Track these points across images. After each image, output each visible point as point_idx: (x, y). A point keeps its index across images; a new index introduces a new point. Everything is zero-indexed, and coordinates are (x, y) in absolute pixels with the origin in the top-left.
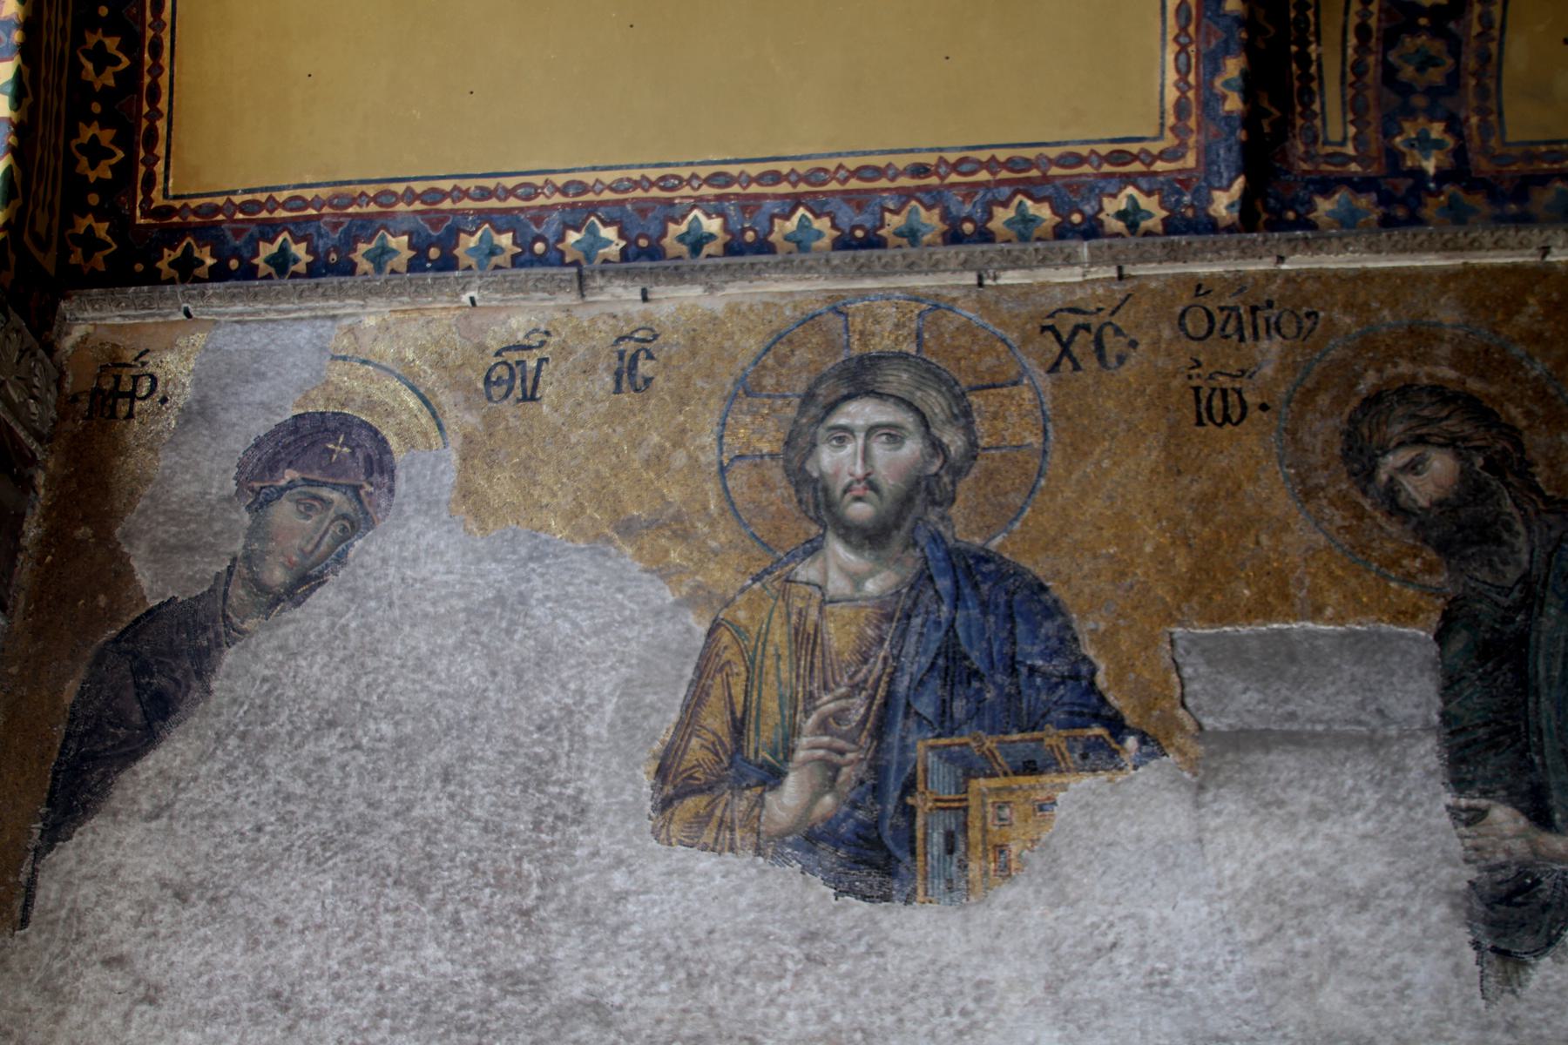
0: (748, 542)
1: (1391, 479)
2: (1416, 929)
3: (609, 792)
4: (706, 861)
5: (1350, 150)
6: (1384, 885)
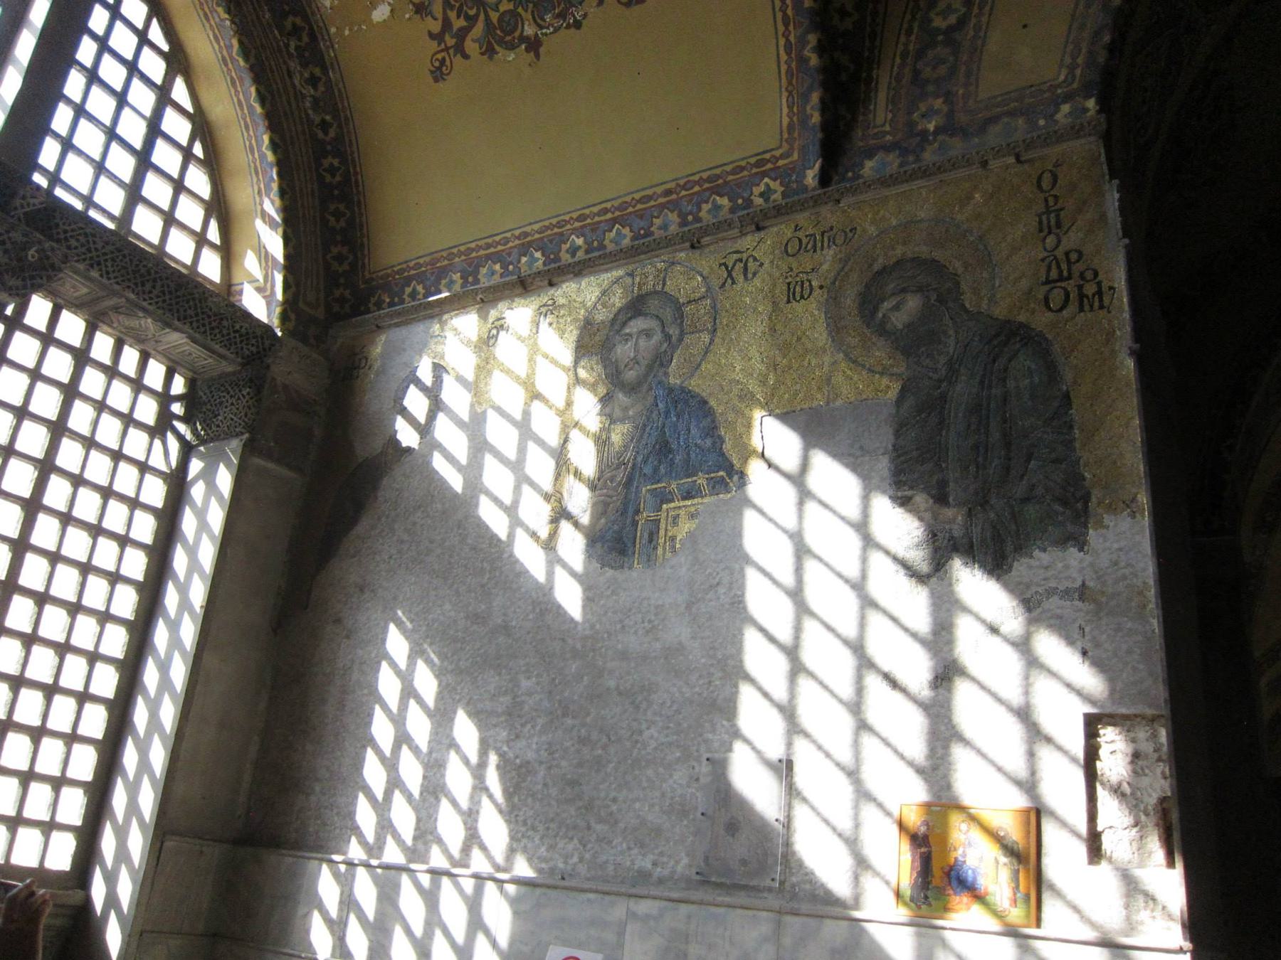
1: (884, 316)
5: (887, 128)
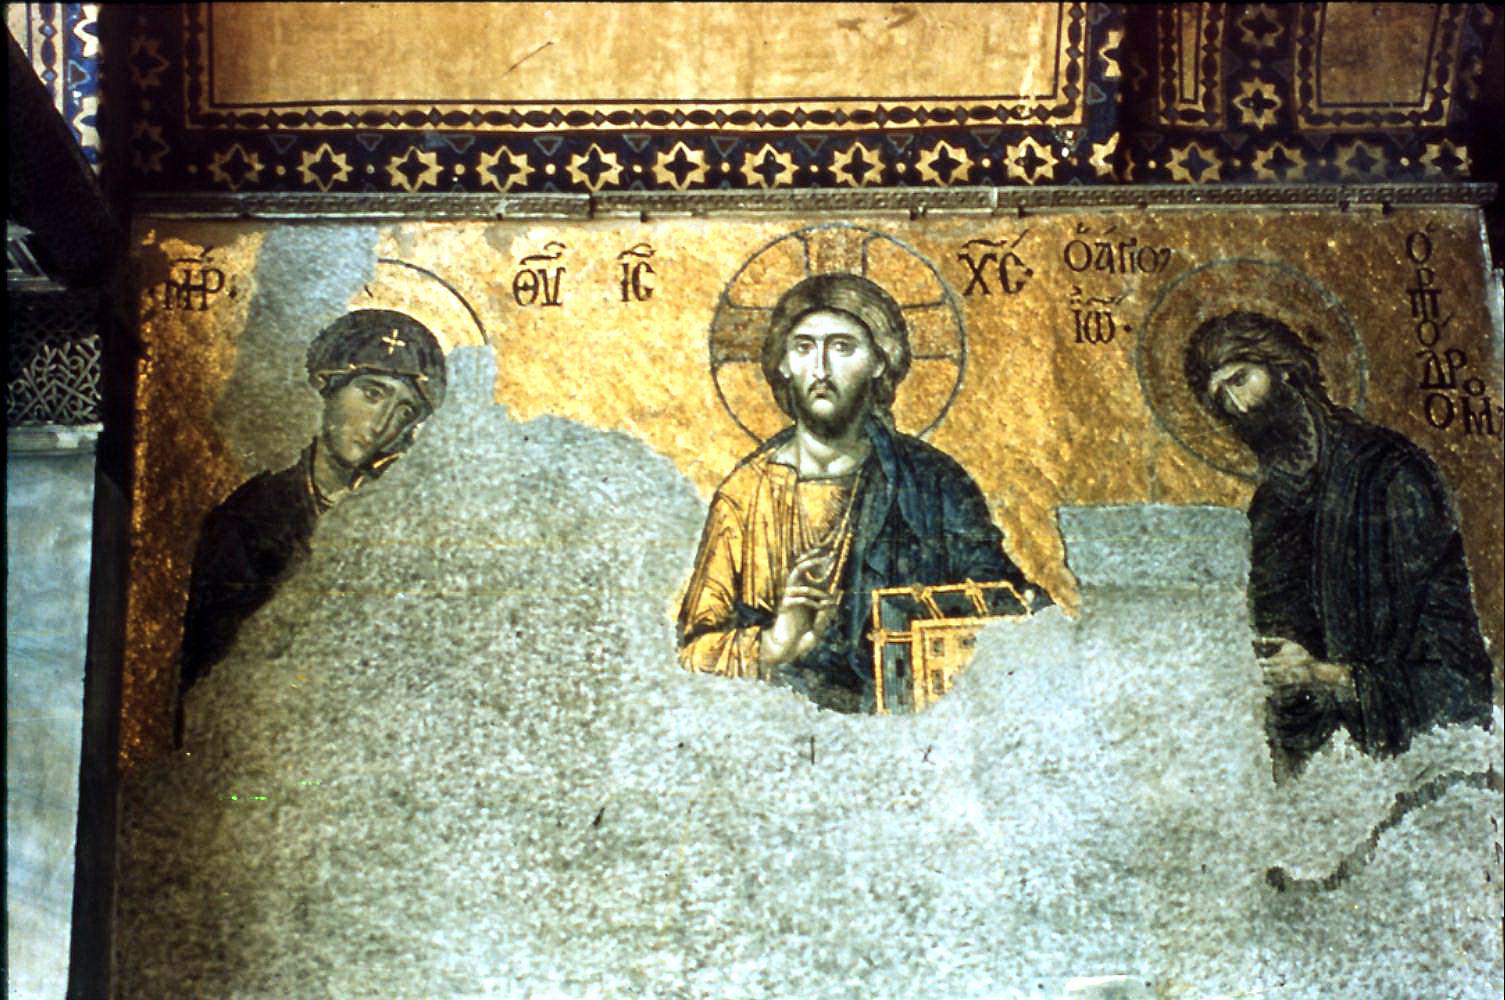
0: (738, 431)
1: (1220, 389)
2: (1229, 732)
3: (643, 631)
4: (720, 684)
5: (1200, 107)
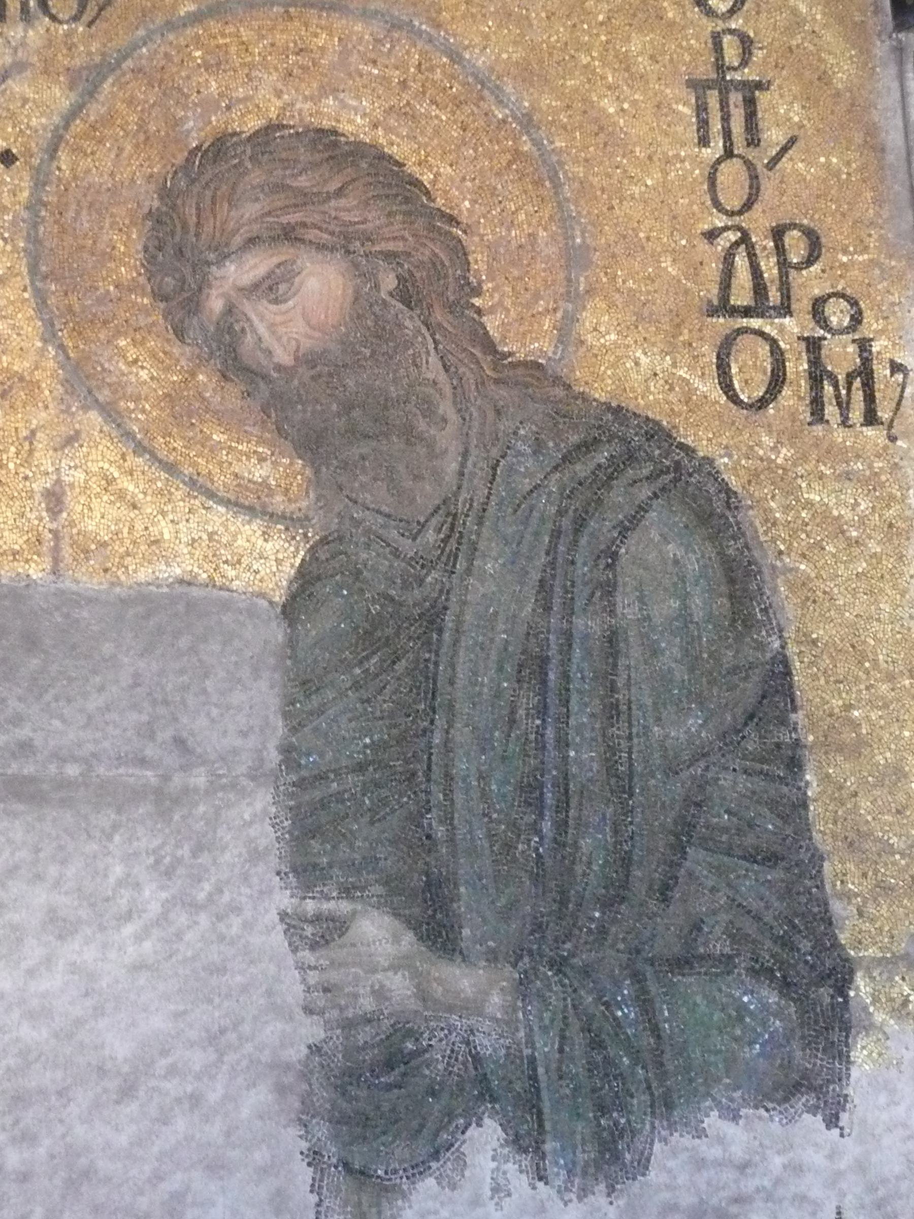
1: (230, 310)
2: (214, 1131)
6: (164, 1053)
